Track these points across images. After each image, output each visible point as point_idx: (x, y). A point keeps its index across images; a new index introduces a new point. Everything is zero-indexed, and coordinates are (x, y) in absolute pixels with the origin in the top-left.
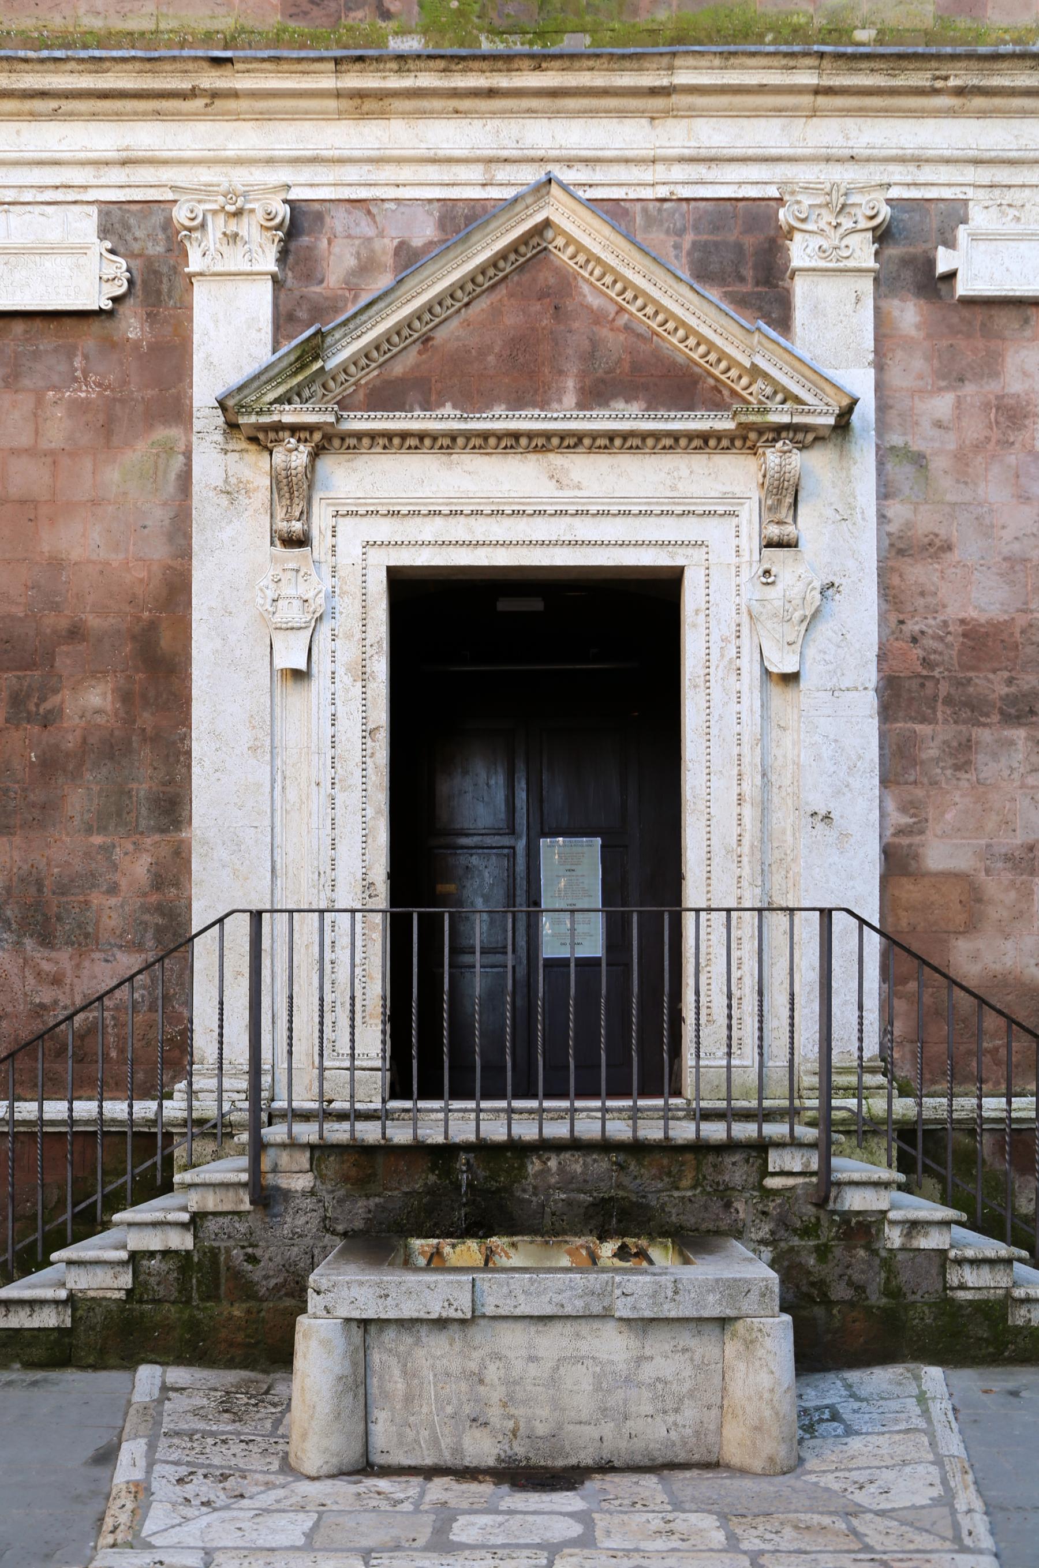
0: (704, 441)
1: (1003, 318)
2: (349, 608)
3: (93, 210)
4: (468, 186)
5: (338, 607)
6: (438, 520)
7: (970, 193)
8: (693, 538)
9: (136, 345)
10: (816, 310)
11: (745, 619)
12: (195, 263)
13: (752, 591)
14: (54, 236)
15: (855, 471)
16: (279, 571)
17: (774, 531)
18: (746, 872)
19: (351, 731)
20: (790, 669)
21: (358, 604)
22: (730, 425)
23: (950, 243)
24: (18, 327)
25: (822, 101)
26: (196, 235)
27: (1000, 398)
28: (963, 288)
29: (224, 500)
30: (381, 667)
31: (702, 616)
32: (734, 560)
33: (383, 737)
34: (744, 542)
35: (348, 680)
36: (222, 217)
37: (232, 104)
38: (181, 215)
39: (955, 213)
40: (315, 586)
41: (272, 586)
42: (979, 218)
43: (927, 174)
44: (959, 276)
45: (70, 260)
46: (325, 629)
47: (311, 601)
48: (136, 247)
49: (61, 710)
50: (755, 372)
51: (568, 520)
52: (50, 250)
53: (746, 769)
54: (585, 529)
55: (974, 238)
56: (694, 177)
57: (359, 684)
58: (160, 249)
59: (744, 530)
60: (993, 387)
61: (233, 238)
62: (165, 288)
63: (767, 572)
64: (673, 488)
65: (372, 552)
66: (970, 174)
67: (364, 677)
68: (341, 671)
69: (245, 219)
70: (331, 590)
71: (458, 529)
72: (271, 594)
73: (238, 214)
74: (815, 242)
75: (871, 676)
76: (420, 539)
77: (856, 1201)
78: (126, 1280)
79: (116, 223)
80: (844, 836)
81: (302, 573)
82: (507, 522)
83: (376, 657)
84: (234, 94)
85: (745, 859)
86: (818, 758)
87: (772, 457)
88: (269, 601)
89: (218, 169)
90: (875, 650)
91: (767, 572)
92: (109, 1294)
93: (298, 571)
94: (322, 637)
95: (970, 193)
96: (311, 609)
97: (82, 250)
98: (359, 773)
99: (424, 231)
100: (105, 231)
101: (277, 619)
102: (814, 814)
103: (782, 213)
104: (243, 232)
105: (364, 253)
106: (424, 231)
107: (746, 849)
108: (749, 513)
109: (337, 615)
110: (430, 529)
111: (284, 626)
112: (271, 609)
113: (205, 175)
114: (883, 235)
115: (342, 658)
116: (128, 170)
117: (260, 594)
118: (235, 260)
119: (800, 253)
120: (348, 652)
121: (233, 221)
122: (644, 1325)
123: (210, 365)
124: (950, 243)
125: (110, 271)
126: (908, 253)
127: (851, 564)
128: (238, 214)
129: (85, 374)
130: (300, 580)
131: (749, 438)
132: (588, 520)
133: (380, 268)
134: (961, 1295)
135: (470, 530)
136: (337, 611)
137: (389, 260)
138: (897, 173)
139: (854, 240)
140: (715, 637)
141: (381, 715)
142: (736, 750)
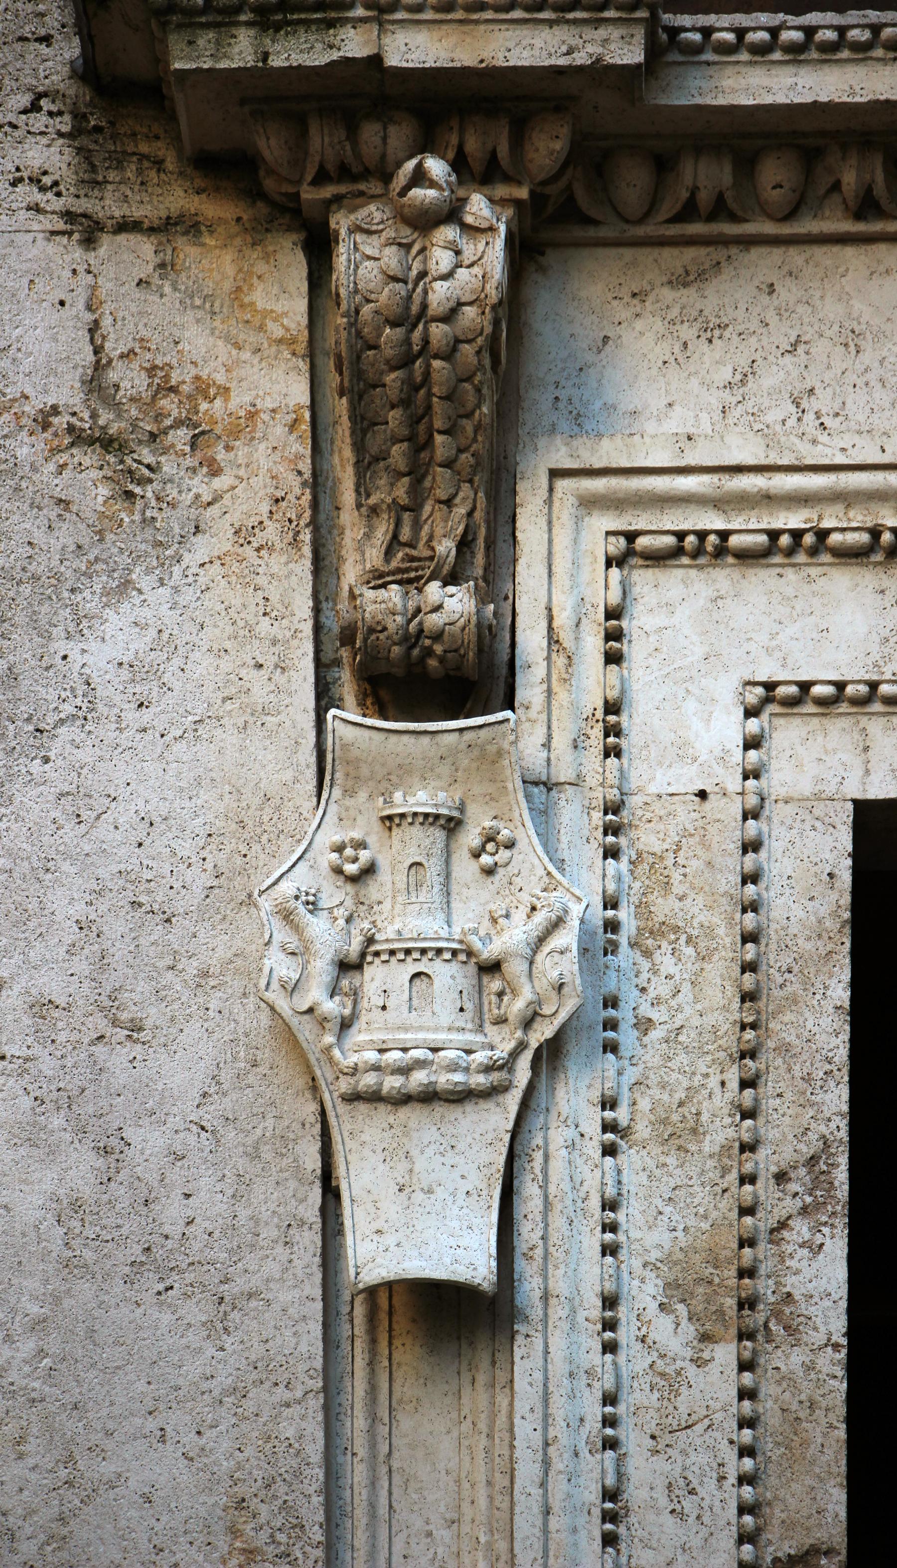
2: (682, 998)
5: (629, 997)
16: (365, 827)
35: (672, 1335)
40: (534, 900)
41: (334, 894)
46: (575, 1100)
47: (516, 968)
57: (725, 1354)
67: (749, 1319)
68: (643, 1294)
70: (598, 915)
72: (326, 935)
81: (471, 837)
83: (801, 1229)
88: (321, 969)
93: (452, 825)
94: (559, 1136)
96: (517, 1006)
101: (359, 1050)
109: (627, 1037)
111: (392, 1083)
112: (331, 1007)
115: (649, 1233)
117: (281, 934)
120: (671, 1208)
130: (465, 869)
136: (624, 1014)
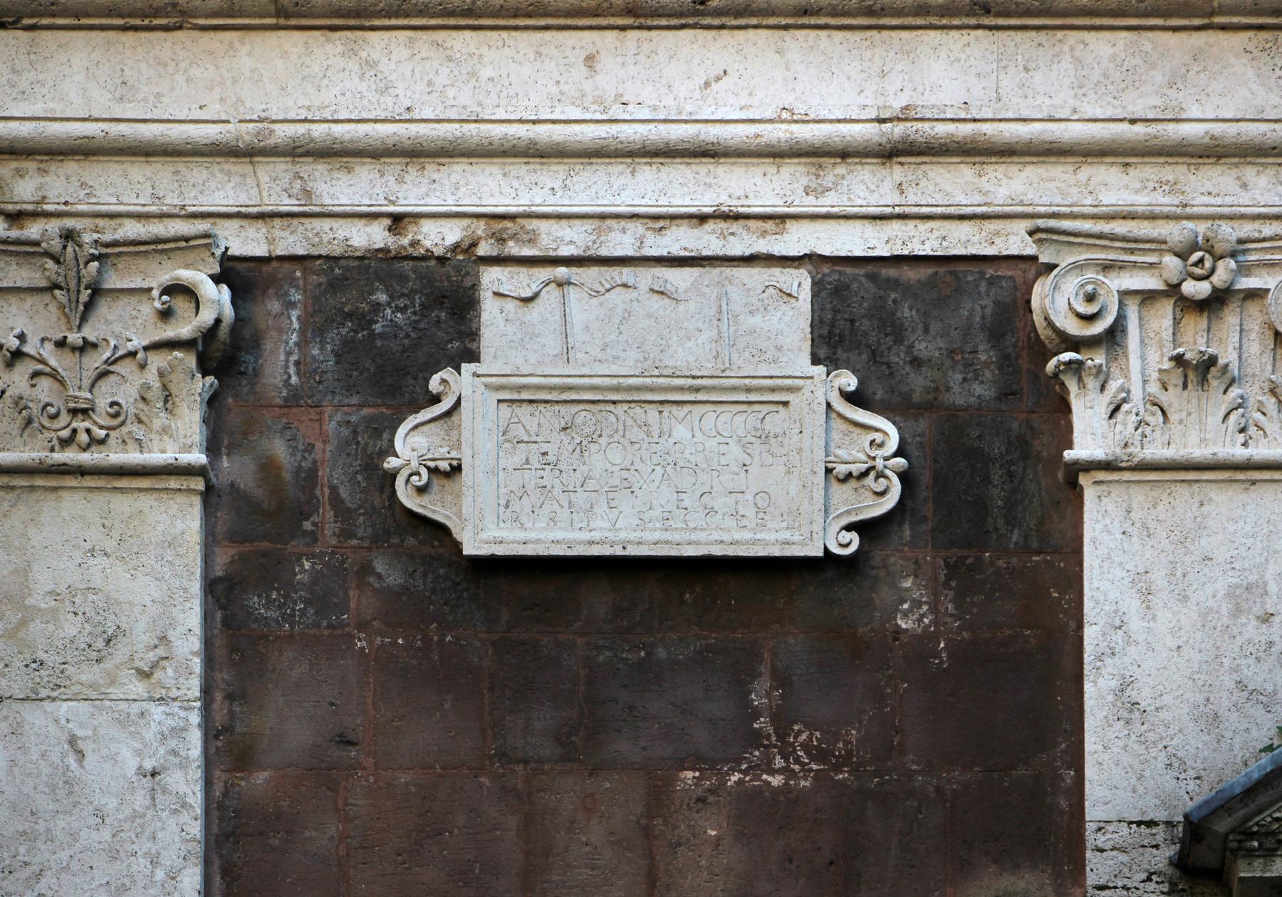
3: (800, 282)
12: (1091, 435)
14: (690, 353)
24: (598, 600)
26: (1098, 358)
36: (1164, 315)
38: (1056, 302)
45: (739, 422)
48: (918, 383)
52: (688, 394)
58: (982, 390)
61: (1199, 371)
62: (997, 495)
69: (1231, 317)
73: (1216, 302)
79: (861, 314)
89: (1149, 172)
97: (777, 395)
100: (829, 345)
104: (1228, 356)
113: (1115, 188)
116: (897, 172)
121: (1195, 326)
125: (853, 453)
128: (1216, 302)
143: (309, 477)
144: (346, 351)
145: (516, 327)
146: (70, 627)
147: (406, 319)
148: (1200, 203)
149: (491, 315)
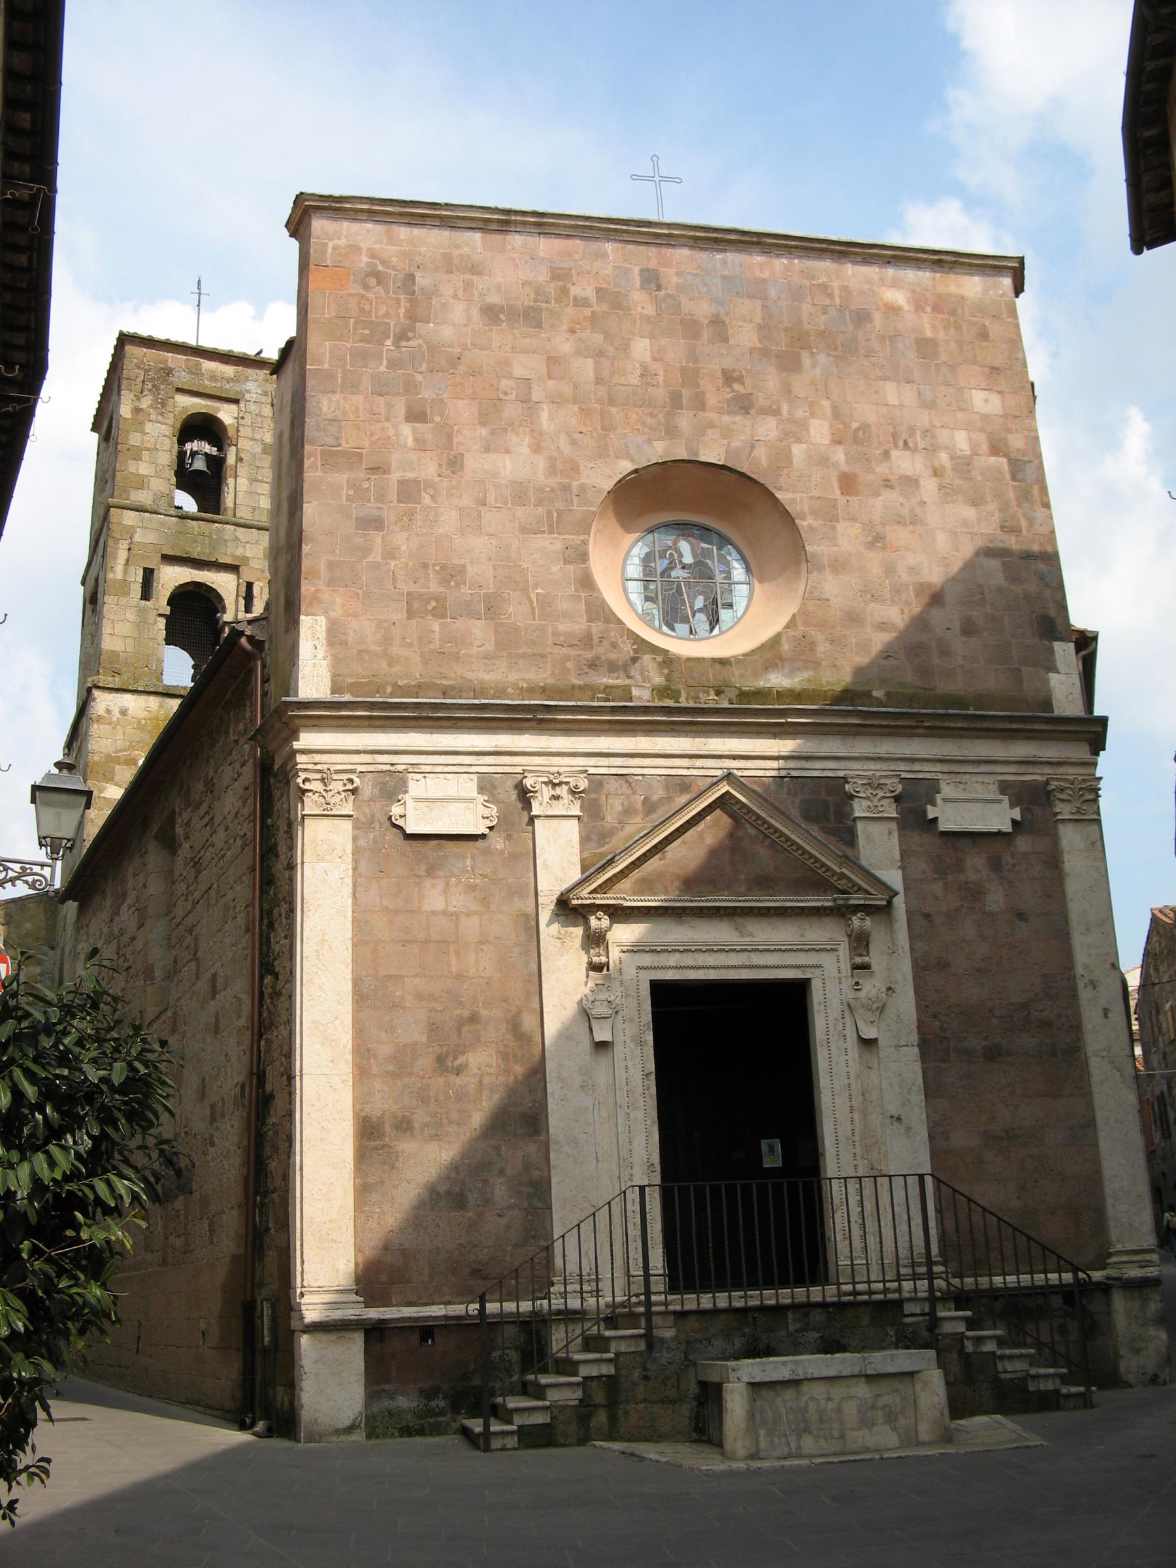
0: (817, 912)
1: (963, 843)
3: (474, 777)
4: (680, 768)
6: (677, 954)
7: (940, 776)
8: (815, 963)
9: (502, 852)
10: (869, 839)
11: (846, 1008)
13: (850, 994)
14: (452, 792)
15: (896, 926)
17: (858, 960)
18: (858, 1151)
19: (636, 1076)
20: (872, 1036)
21: (635, 1002)
22: (830, 904)
23: (934, 804)
25: (861, 729)
27: (966, 883)
28: (943, 826)
29: (558, 943)
30: (650, 1038)
31: (822, 1007)
32: (836, 974)
33: (653, 1077)
34: (842, 964)
35: (632, 1046)
37: (553, 725)
39: (933, 787)
42: (947, 790)
43: (917, 767)
44: (940, 820)
49: (466, 1065)
50: (842, 876)
51: (746, 954)
53: (854, 1093)
54: (757, 959)
55: (945, 800)
56: (800, 766)
59: (841, 958)
60: (962, 877)
61: (556, 798)
63: (857, 983)
64: (802, 936)
65: (641, 972)
66: (939, 767)
67: (642, 1043)
71: (688, 960)
73: (560, 784)
74: (865, 803)
75: (914, 1038)
76: (668, 964)
77: (948, 1328)
78: (579, 1394)
80: (908, 1128)
82: (714, 955)
84: (555, 720)
85: (857, 1143)
86: (891, 1085)
87: (856, 921)
90: (916, 1023)
91: (857, 983)
92: (570, 1403)
95: (940, 776)
98: (642, 1099)
99: (658, 793)
100: (481, 789)
102: (892, 1117)
103: (847, 786)
105: (626, 803)
106: (658, 793)
107: (857, 1138)
108: (844, 949)
110: (672, 960)
114: (897, 799)
115: (628, 1033)
118: (558, 809)
119: (859, 809)
120: (630, 1030)
122: (870, 1378)
123: (546, 866)
124: (934, 804)
125: (487, 813)
126: (912, 807)
127: (899, 977)
129: (473, 867)
131: (841, 912)
132: (758, 954)
133: (635, 812)
134: (1003, 1376)
135: (695, 959)
137: (639, 807)
138: (903, 766)
139: (885, 802)
140: (830, 1018)
141: (651, 1066)
142: (847, 1081)
143: (373, 816)
144: (381, 790)
145: (416, 787)
146: (325, 847)
147: (392, 785)
148: (555, 763)
149: (412, 785)
